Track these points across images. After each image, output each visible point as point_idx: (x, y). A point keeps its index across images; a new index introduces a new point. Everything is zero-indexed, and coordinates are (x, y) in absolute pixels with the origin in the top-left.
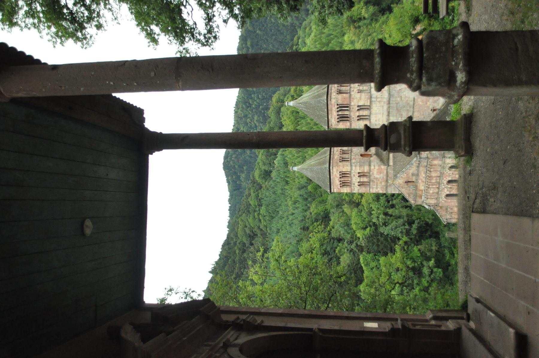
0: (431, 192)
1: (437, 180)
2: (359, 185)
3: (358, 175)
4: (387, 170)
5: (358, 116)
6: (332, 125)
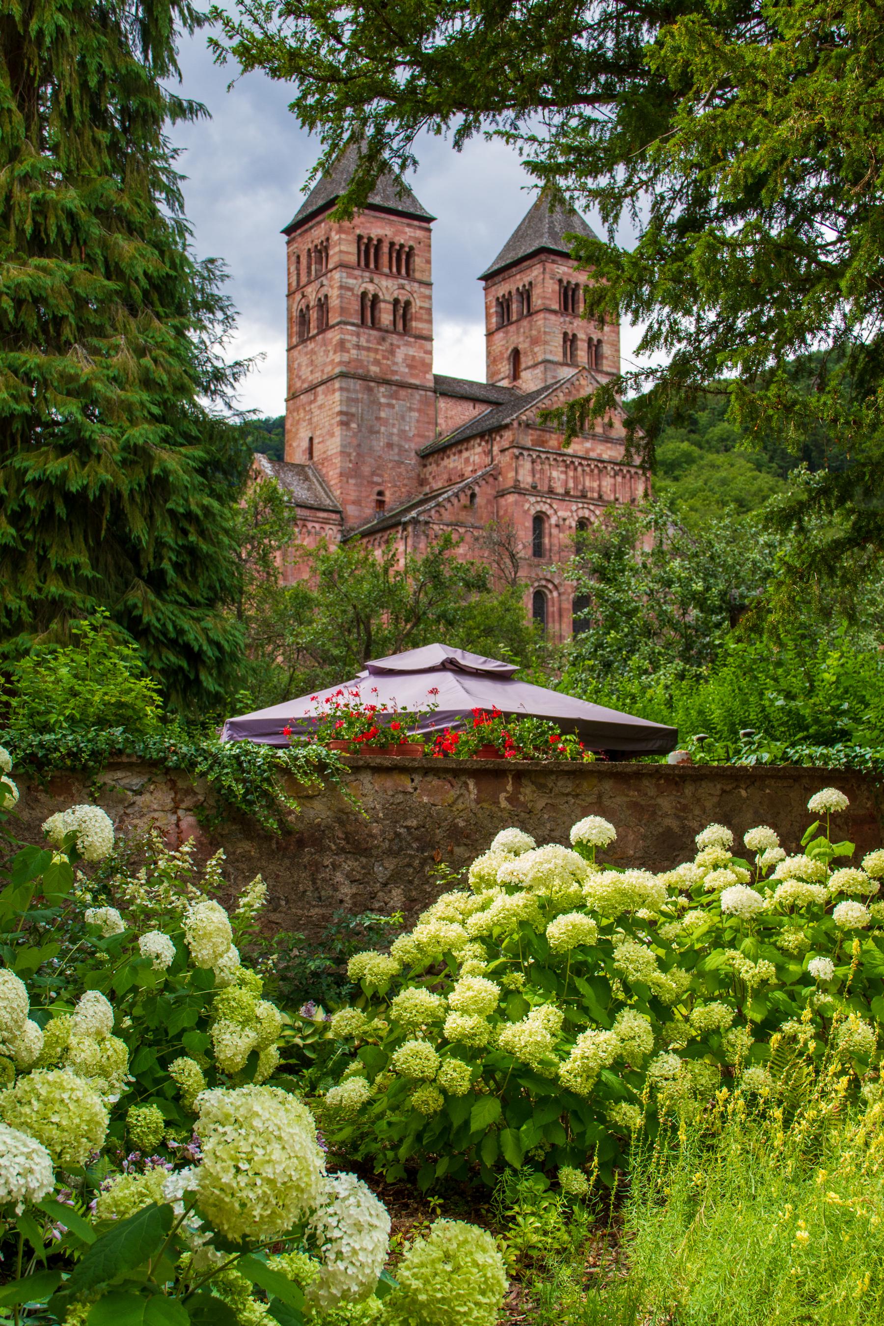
0: (555, 474)
1: (592, 490)
2: (364, 295)
3: (403, 299)
4: (425, 389)
5: (574, 336)
6: (553, 262)
